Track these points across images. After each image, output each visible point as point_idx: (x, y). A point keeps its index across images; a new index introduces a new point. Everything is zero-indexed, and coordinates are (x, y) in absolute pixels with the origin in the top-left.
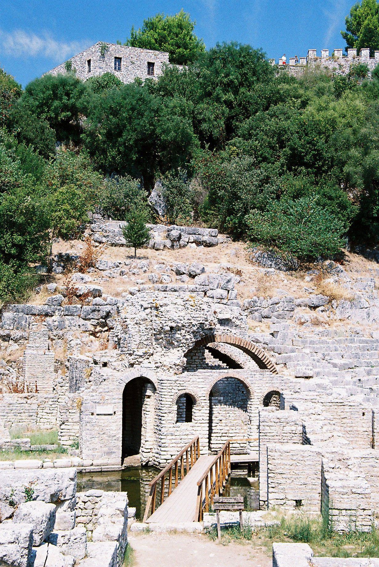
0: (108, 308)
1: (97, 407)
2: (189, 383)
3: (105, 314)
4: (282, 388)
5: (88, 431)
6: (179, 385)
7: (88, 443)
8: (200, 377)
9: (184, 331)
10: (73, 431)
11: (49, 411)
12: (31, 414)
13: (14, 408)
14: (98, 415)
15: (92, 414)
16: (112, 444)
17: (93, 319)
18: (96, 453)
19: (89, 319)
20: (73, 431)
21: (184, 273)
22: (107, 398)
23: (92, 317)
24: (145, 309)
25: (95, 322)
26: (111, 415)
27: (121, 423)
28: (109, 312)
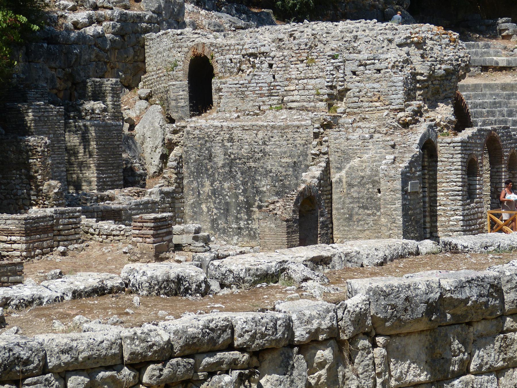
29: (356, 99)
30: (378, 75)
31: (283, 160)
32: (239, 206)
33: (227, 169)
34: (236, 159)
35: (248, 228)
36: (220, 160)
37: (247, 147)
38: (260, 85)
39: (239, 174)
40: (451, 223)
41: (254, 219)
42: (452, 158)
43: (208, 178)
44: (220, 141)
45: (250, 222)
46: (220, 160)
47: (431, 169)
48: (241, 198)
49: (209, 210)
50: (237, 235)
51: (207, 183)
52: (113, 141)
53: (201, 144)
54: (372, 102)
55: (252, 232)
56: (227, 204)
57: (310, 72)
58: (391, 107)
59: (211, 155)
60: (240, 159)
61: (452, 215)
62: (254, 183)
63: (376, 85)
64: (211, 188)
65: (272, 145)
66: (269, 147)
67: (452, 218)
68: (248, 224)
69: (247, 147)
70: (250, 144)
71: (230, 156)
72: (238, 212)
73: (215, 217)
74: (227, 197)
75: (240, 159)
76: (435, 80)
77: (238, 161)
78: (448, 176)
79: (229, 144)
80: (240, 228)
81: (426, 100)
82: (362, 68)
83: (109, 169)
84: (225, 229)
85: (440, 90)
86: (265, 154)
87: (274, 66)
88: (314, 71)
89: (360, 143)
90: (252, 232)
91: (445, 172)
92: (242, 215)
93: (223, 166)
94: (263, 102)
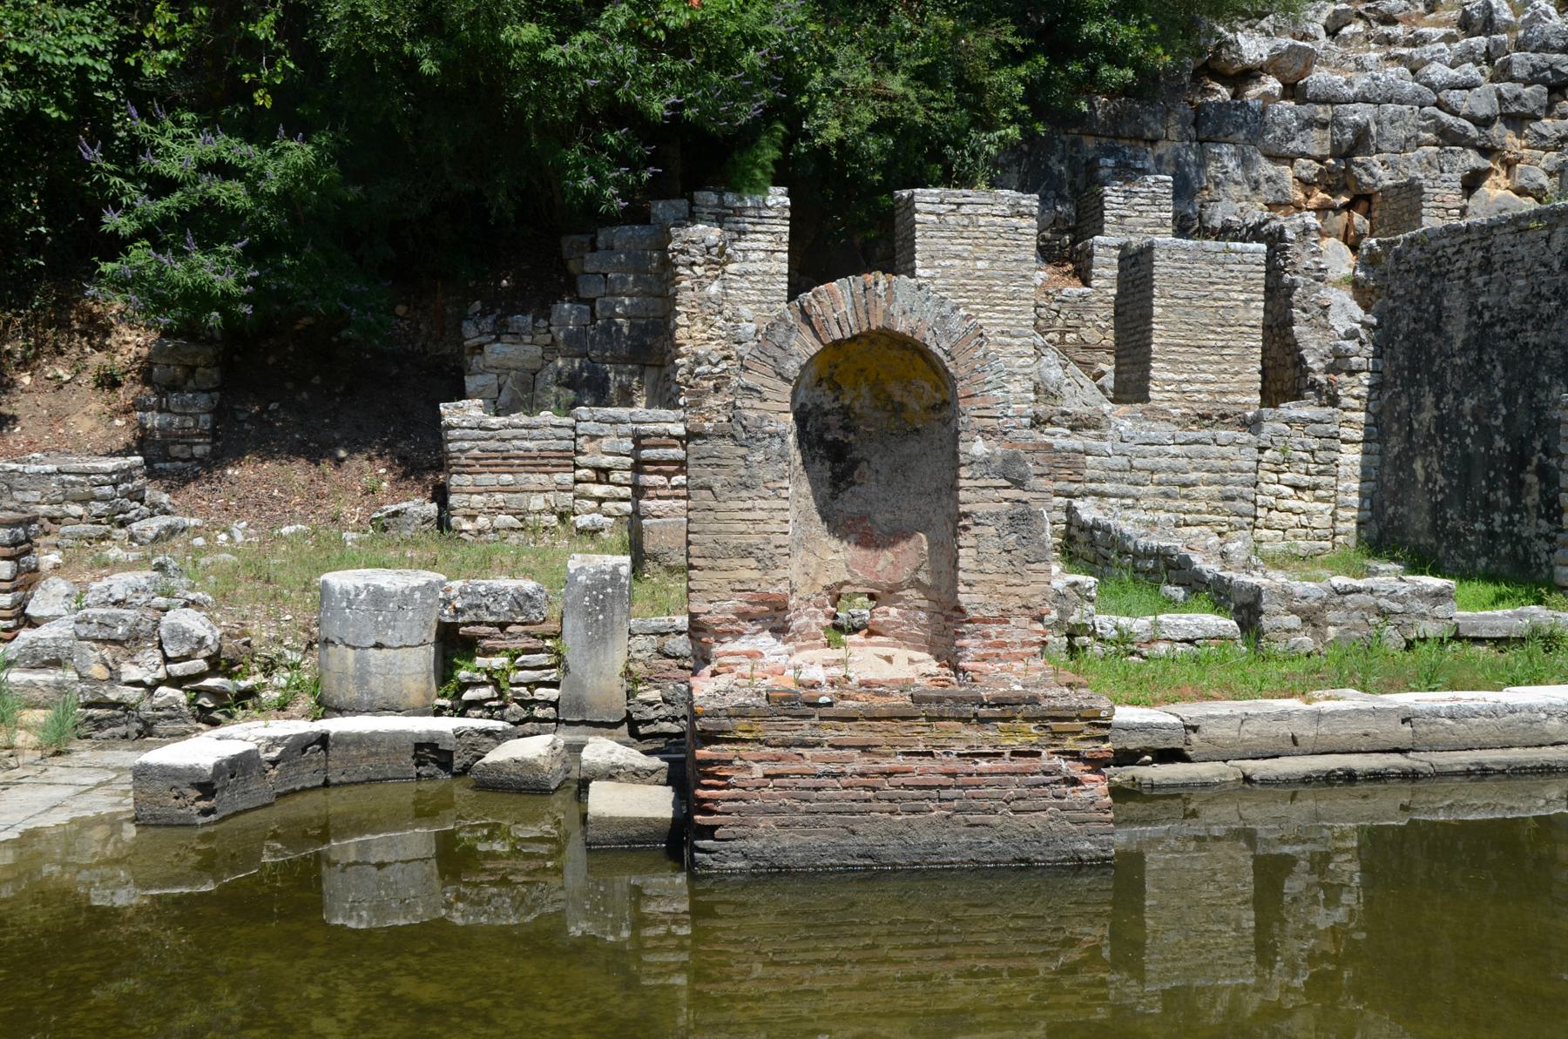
0: (1361, 114)
3: (1349, 136)
13: (1164, 462)
19: (1290, 159)
23: (1302, 148)
25: (1309, 169)
32: (1492, 467)
33: (1473, 354)
34: (1492, 325)
35: (1511, 533)
36: (1458, 331)
37: (1521, 283)
39: (1499, 368)
41: (1526, 508)
43: (1430, 384)
44: (1462, 272)
45: (1517, 517)
46: (1458, 331)
48: (1500, 442)
49: (1428, 478)
50: (1485, 554)
51: (1429, 400)
52: (1226, 291)
53: (1422, 287)
55: (1520, 549)
56: (1467, 457)
59: (1439, 317)
60: (1503, 322)
62: (1531, 396)
64: (1436, 413)
68: (1511, 522)
69: (1521, 283)
70: (1530, 274)
71: (1480, 315)
72: (1492, 488)
73: (1440, 498)
74: (1468, 441)
75: (1503, 322)
77: (1497, 329)
79: (1479, 281)
80: (1491, 534)
83: (1204, 362)
90: (1520, 549)
92: (1500, 493)
93: (1464, 349)
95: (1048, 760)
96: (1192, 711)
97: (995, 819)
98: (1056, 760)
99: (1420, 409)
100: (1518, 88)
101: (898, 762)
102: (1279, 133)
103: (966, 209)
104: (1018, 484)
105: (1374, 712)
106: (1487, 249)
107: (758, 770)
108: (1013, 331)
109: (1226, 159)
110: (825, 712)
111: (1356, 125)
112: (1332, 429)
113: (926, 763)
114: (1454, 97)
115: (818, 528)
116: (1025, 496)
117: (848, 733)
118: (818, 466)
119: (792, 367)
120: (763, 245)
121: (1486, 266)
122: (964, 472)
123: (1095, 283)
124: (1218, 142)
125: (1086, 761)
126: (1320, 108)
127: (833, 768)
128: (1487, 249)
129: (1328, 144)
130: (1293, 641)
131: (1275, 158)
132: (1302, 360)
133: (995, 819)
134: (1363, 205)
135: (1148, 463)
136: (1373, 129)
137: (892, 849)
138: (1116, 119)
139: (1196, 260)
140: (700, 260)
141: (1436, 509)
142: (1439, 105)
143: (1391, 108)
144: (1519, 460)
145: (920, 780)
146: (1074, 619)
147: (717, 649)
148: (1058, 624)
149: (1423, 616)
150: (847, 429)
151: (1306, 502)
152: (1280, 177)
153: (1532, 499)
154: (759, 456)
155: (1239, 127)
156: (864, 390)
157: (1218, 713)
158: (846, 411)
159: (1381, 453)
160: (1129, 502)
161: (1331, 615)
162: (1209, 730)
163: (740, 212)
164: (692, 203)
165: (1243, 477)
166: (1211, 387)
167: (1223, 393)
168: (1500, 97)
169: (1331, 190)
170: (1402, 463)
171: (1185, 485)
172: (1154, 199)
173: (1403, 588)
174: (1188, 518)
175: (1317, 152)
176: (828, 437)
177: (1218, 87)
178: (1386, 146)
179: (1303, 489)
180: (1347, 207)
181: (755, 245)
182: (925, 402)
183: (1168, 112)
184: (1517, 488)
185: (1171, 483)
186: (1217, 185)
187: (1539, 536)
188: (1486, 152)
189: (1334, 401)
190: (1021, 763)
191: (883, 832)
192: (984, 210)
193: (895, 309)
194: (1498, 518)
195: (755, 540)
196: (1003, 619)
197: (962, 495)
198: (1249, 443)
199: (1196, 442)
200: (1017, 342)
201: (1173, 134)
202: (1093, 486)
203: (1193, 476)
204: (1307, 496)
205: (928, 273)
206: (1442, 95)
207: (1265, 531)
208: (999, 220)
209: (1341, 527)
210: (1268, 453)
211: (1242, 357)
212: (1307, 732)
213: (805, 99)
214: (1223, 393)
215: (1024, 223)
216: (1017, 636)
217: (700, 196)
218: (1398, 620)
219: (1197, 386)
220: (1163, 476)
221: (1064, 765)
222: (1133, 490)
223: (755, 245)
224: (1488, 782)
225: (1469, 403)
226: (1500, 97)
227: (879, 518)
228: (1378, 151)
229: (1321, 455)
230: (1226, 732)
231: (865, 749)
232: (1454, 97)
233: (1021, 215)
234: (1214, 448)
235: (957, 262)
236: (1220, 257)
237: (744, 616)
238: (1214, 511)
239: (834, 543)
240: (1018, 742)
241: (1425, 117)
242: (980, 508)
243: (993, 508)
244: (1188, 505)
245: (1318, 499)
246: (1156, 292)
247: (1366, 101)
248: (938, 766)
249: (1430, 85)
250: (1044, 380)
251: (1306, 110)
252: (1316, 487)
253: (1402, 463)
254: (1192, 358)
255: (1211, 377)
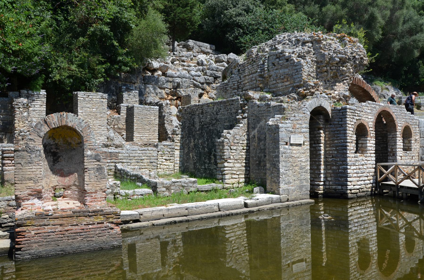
0: (178, 80)
1: (292, 136)
2: (363, 113)
3: (176, 84)
4: (411, 123)
5: (283, 163)
6: (356, 115)
7: (283, 175)
8: (369, 108)
9: (349, 64)
10: (234, 169)
11: (168, 158)
12: (152, 161)
13: (137, 155)
14: (291, 145)
15: (287, 144)
16: (303, 177)
17: (167, 88)
18: (291, 187)
19: (164, 89)
20: (234, 169)
21: (223, 61)
22: (298, 126)
23: (166, 86)
24: (304, 43)
25: (168, 91)
26: (300, 145)
27: (309, 154)
28: (179, 83)
29: (275, 82)
30: (286, 63)
31: (225, 124)
32: (205, 155)
33: (201, 131)
36: (197, 126)
38: (233, 83)
40: (340, 171)
41: (212, 163)
42: (341, 121)
46: (197, 126)
47: (327, 130)
48: (206, 149)
49: (193, 157)
51: (192, 141)
53: (190, 117)
54: (283, 82)
56: (200, 153)
57: (253, 69)
58: (295, 84)
59: (194, 123)
60: (206, 125)
61: (341, 165)
62: (212, 140)
63: (286, 70)
65: (221, 114)
66: (219, 116)
67: (341, 167)
68: (209, 166)
69: (209, 117)
70: (210, 115)
75: (206, 125)
76: (333, 66)
78: (338, 135)
79: (201, 116)
80: (205, 169)
81: (327, 81)
82: (277, 60)
84: (199, 169)
85: (338, 74)
86: (217, 120)
87: (241, 70)
88: (255, 68)
89: (265, 108)
91: (336, 132)
93: (199, 130)
94: (235, 93)
95: (106, 224)
96: (141, 211)
97: (94, 239)
98: (108, 224)
99: (191, 143)
100: (208, 77)
101: (69, 227)
102: (161, 83)
103: (90, 97)
104: (99, 161)
105: (180, 208)
106: (202, 110)
107: (33, 233)
108: (102, 125)
109: (150, 88)
110: (50, 217)
111: (177, 82)
112: (173, 147)
113: (77, 227)
114: (196, 78)
115: (50, 173)
116: (100, 164)
117: (56, 221)
118: (49, 158)
119: (42, 134)
120: (39, 104)
121: (202, 113)
122: (85, 158)
123: (121, 114)
124: (148, 84)
125: (115, 224)
126: (170, 78)
127: (53, 230)
128: (202, 110)
129: (172, 86)
130: (164, 194)
131: (161, 88)
132: (167, 132)
133: (94, 239)
134: (179, 99)
135: (133, 155)
136: (181, 83)
137: (68, 248)
138: (126, 78)
139: (143, 110)
140: (21, 107)
141: (195, 164)
142: (193, 79)
143: (184, 79)
144: (210, 153)
145: (75, 231)
146: (115, 191)
147: (23, 203)
148: (111, 193)
149: (191, 187)
150: (57, 149)
151: (168, 163)
152: (162, 92)
153: (213, 161)
154: (34, 156)
155: (153, 81)
156: (61, 139)
157: (147, 211)
158: (56, 144)
159: (183, 152)
160: (129, 164)
161: (172, 188)
162: (145, 215)
163: (33, 95)
164: (20, 92)
165: (154, 158)
166: (147, 138)
167: (150, 139)
168: (205, 79)
169: (173, 96)
170: (188, 154)
171: (142, 160)
172: (134, 96)
173: (187, 181)
174: (143, 167)
175: (169, 87)
176: (52, 151)
177: (148, 72)
178: (183, 87)
179: (167, 160)
180: (176, 99)
181: (37, 104)
182: (76, 142)
183: (137, 77)
184: (210, 159)
185: (138, 159)
186: (148, 93)
187: (214, 169)
188: (203, 89)
189: (173, 141)
190: (99, 225)
191: (66, 245)
192: (95, 97)
193: (68, 121)
194: (206, 165)
195: (33, 176)
196: (96, 192)
197: (85, 164)
198: (155, 150)
199: (144, 150)
200: (103, 127)
201: (138, 82)
202: (121, 160)
203: (143, 158)
204: (168, 161)
205: (81, 111)
206: (194, 77)
207: (160, 170)
208: (98, 100)
209: (176, 168)
210: (160, 152)
211: (154, 131)
212: (166, 213)
213: (50, 69)
214: (150, 139)
215: (104, 100)
216: (99, 196)
217: (22, 91)
218: (186, 188)
219: (144, 138)
220: (137, 158)
221: (110, 225)
222: (130, 161)
223: (37, 104)
224: (203, 221)
225: (200, 141)
226: (205, 79)
227: (65, 170)
228: (182, 88)
229: (171, 153)
230: (148, 215)
231: (61, 225)
232: (196, 78)
233: (103, 99)
234: (148, 151)
235: (88, 109)
236: (149, 109)
237: (30, 195)
238: (148, 165)
239: (54, 176)
240: (98, 221)
241: (191, 82)
242: (90, 167)
243: (93, 167)
244: (142, 164)
245: (171, 162)
246: (135, 117)
247: (179, 77)
248: (79, 228)
249: (192, 75)
250: (110, 136)
251: (167, 79)
252: (170, 160)
253: (188, 154)
254: (143, 131)
255: (147, 136)
